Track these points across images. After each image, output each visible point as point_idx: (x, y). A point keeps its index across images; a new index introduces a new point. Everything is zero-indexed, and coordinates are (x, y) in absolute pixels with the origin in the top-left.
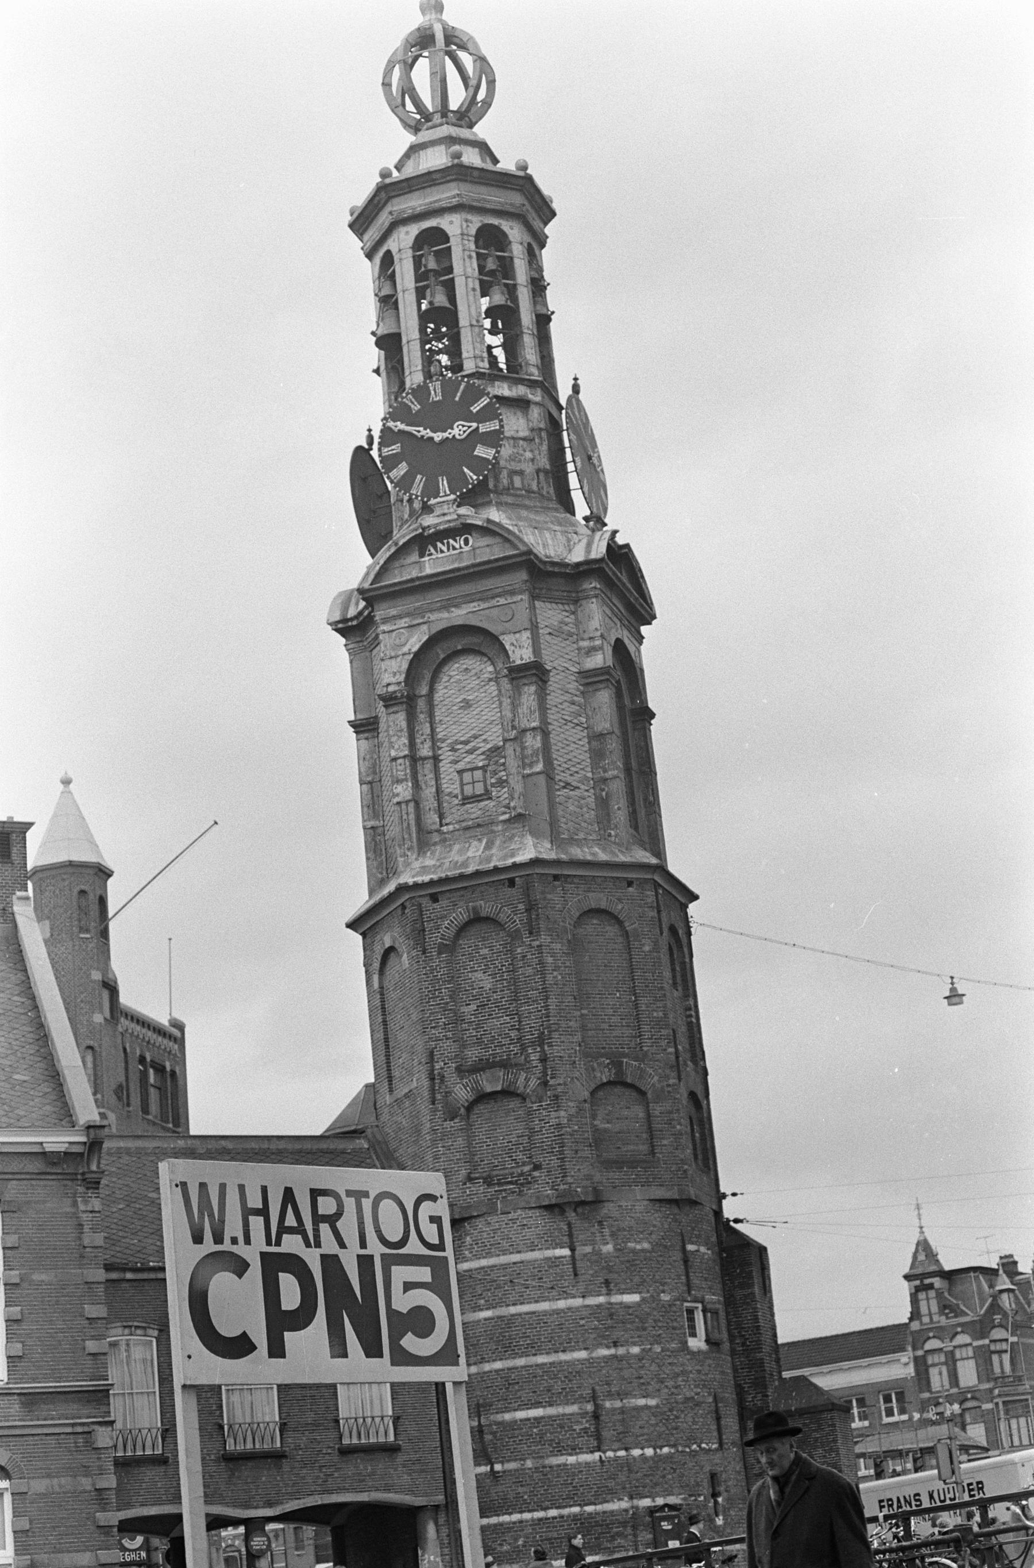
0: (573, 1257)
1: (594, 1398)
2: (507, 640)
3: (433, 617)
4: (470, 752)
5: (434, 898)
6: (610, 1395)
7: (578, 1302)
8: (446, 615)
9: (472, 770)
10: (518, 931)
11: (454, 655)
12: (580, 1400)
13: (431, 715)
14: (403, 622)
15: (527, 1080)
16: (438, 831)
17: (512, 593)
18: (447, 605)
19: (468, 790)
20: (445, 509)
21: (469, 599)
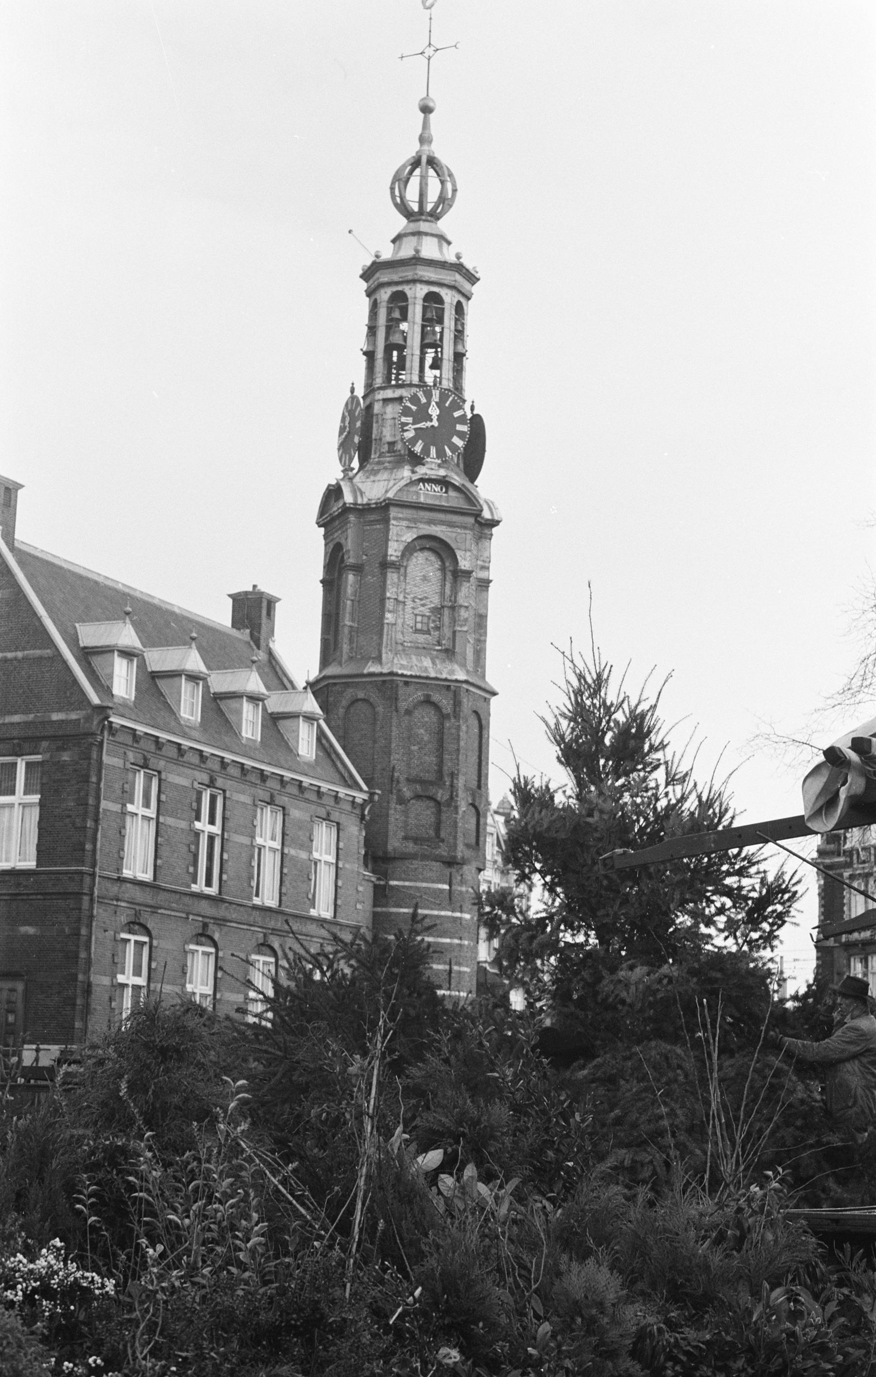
0: (450, 890)
1: (450, 964)
2: (459, 554)
3: (421, 526)
4: (423, 605)
5: (406, 683)
6: (456, 964)
7: (449, 913)
8: (427, 527)
9: (423, 616)
10: (449, 714)
11: (422, 549)
12: (445, 963)
13: (405, 576)
14: (405, 523)
15: (443, 795)
16: (402, 644)
17: (465, 528)
18: (431, 522)
19: (419, 626)
20: (433, 466)
21: (442, 523)
